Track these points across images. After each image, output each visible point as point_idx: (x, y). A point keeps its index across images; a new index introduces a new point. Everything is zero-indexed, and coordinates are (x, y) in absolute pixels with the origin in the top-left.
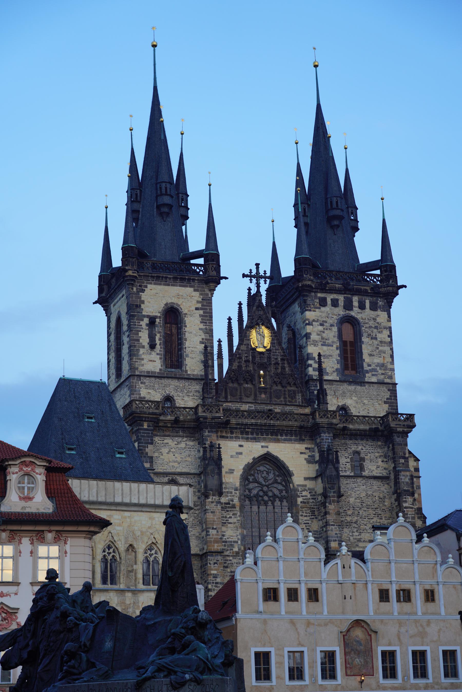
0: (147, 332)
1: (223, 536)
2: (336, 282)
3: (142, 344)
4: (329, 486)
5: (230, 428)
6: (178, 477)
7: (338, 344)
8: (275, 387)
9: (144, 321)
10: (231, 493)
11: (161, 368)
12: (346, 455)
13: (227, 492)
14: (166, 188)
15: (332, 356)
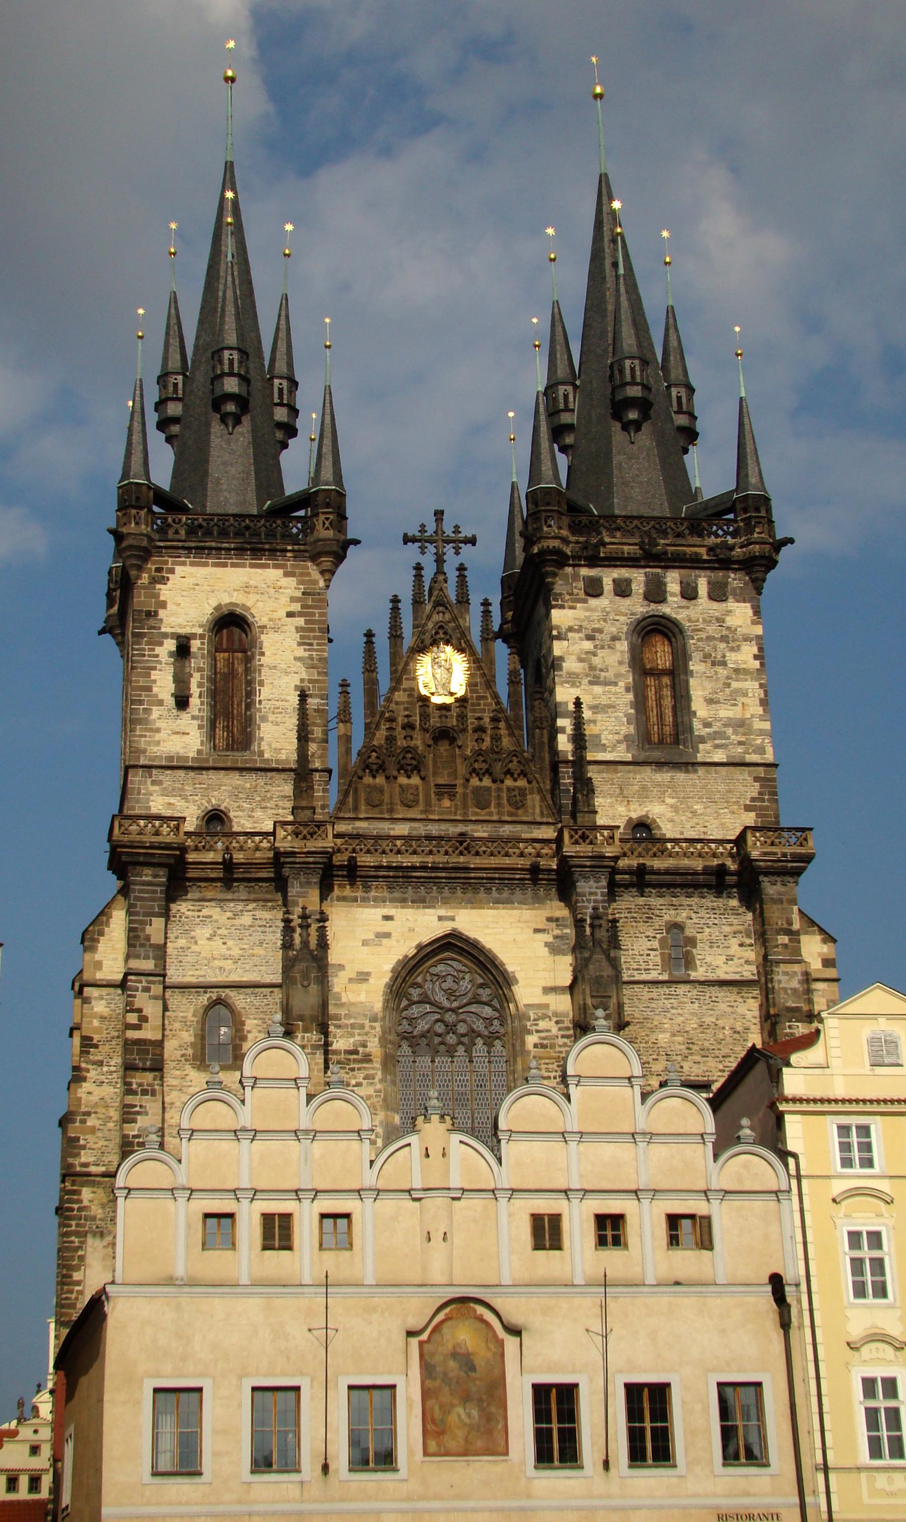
0: (171, 669)
2: (624, 541)
3: (157, 696)
4: (595, 1003)
6: (231, 993)
7: (631, 680)
8: (475, 781)
9: (165, 645)
10: (362, 1027)
11: (200, 748)
12: (648, 933)
13: (353, 1026)
14: (231, 362)
15: (614, 707)
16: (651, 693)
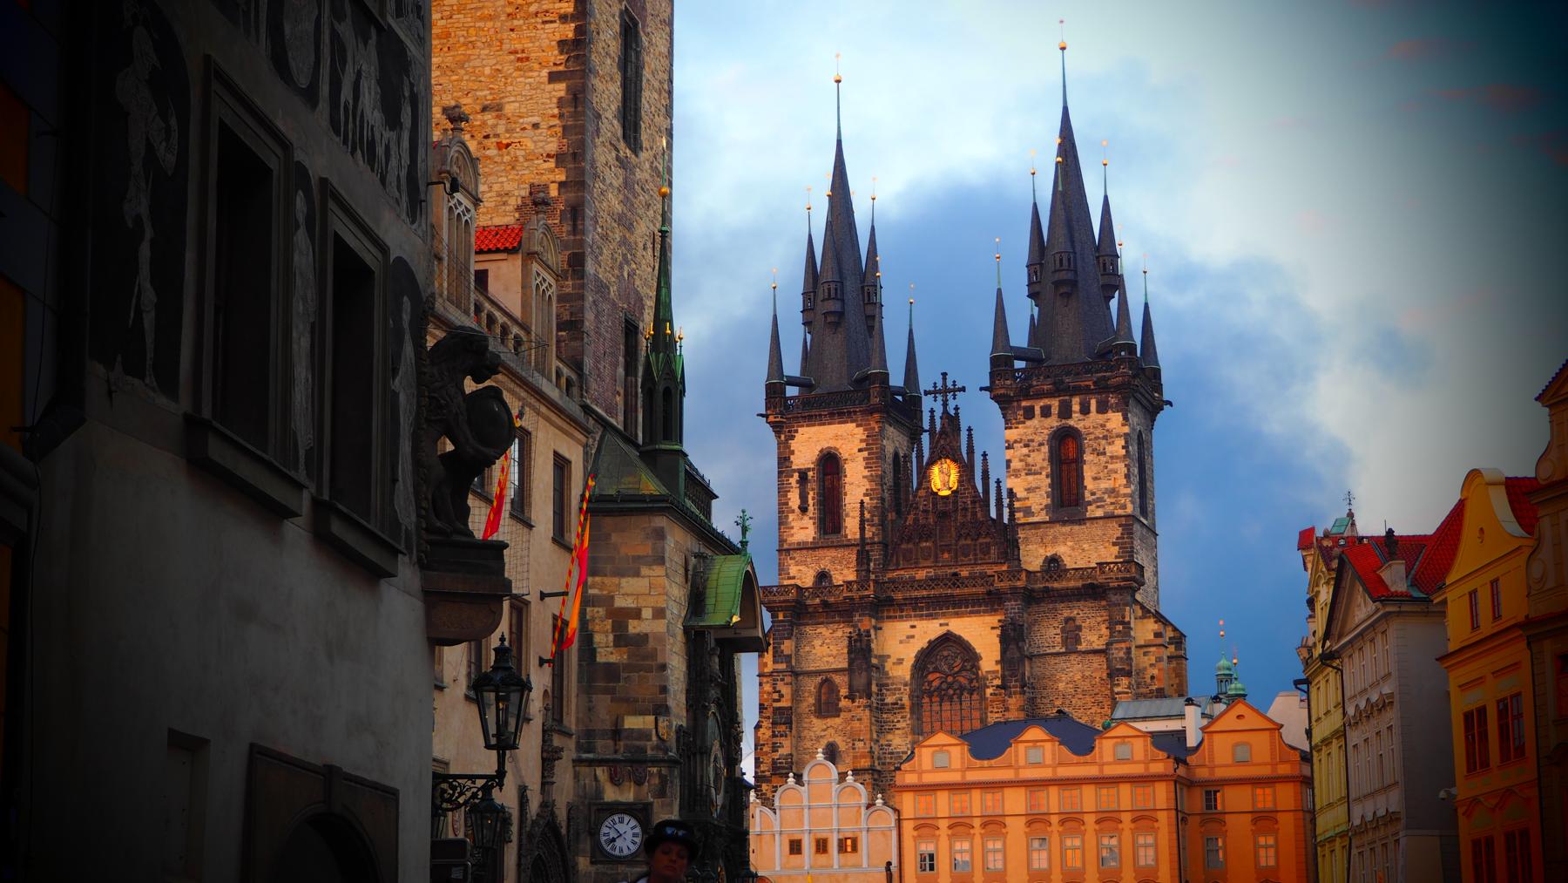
5: (899, 605)
8: (963, 542)
16: (1064, 474)
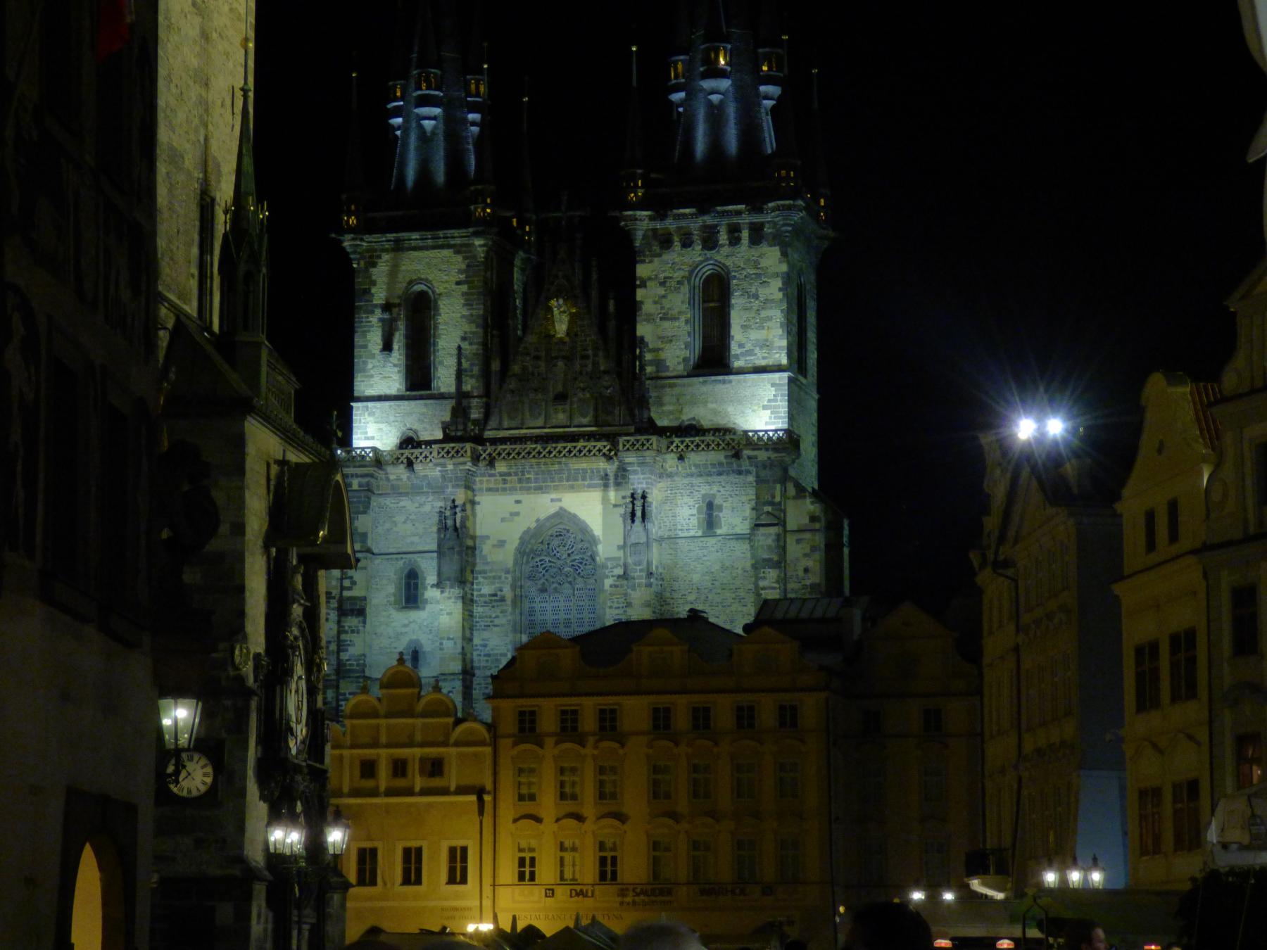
1: (485, 646)
5: (501, 475)
13: (494, 577)
